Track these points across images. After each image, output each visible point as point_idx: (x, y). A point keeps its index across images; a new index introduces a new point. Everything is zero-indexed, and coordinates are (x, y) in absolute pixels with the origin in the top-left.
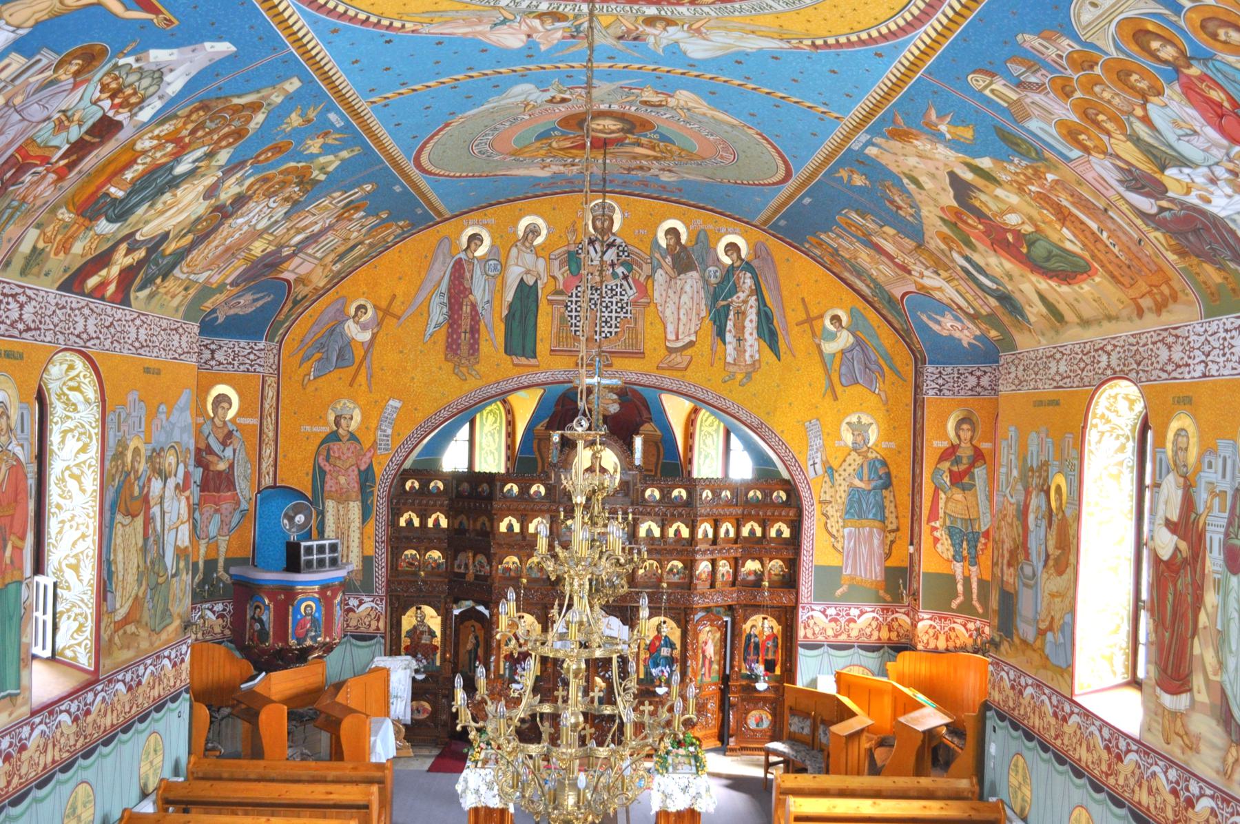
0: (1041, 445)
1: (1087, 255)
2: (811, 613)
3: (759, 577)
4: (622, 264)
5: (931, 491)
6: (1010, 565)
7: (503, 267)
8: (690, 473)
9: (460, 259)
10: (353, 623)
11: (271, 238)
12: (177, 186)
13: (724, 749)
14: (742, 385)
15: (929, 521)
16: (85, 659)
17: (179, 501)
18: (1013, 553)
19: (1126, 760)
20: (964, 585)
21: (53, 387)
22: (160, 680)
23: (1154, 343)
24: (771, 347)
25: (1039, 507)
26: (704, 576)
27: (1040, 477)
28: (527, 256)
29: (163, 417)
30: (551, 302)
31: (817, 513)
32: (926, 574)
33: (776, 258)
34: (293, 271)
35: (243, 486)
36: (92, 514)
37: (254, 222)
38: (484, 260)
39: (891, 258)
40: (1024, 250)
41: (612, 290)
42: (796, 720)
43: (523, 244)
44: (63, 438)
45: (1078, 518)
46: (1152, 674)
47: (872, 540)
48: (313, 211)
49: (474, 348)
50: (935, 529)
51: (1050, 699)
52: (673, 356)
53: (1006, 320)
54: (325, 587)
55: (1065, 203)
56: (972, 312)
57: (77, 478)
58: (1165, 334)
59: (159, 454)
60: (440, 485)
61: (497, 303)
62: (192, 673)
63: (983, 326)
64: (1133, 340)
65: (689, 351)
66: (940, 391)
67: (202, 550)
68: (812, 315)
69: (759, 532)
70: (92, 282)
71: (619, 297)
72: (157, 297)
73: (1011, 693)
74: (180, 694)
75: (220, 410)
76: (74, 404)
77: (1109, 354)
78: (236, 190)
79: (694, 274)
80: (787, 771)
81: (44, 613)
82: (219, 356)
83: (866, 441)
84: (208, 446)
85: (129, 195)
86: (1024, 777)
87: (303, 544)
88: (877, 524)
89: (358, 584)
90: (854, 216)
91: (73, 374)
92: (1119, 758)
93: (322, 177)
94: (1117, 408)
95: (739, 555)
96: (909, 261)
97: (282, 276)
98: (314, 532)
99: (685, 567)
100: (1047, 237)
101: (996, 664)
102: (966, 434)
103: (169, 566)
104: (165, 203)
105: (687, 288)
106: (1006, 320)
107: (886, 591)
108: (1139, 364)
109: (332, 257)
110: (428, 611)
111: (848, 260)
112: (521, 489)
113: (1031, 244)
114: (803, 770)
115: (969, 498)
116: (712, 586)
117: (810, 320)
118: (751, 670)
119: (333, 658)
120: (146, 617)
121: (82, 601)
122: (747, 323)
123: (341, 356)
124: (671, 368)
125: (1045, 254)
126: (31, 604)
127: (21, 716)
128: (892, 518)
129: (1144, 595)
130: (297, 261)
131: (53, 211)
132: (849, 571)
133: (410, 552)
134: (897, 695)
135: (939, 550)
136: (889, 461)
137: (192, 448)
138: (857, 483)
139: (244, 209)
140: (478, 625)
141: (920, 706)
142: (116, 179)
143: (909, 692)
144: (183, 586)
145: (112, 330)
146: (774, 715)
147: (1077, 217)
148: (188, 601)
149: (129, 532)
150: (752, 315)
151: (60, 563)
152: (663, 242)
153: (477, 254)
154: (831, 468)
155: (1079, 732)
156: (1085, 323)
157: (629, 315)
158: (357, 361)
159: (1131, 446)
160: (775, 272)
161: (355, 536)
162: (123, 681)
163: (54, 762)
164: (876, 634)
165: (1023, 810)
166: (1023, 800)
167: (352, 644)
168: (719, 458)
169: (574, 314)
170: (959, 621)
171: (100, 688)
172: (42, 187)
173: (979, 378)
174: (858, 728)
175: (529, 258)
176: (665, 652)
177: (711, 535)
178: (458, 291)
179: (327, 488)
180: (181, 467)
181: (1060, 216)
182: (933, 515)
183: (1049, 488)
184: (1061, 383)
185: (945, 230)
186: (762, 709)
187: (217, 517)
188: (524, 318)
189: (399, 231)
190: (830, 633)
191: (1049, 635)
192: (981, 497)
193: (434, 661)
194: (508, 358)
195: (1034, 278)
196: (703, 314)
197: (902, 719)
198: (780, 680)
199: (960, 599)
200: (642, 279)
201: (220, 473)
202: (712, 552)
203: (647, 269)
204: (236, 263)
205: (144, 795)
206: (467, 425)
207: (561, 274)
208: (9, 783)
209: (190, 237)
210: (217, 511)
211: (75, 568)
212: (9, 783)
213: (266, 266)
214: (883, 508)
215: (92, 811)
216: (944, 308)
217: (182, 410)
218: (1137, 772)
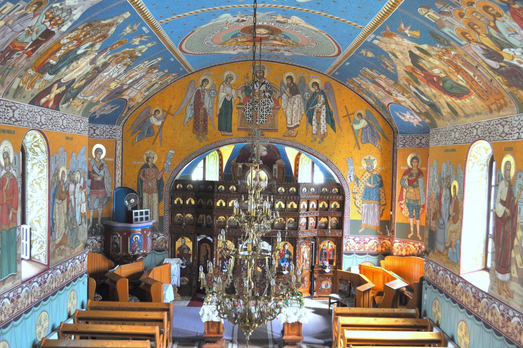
0: (447, 168)
1: (468, 87)
3: (327, 224)
4: (268, 92)
5: (400, 188)
6: (433, 219)
7: (218, 93)
8: (297, 181)
11: (118, 81)
12: (78, 59)
13: (311, 297)
14: (319, 143)
15: (399, 201)
16: (44, 260)
17: (82, 193)
18: (435, 214)
19: (482, 302)
20: (414, 228)
21: (28, 145)
22: (75, 268)
23: (497, 125)
24: (332, 127)
25: (446, 195)
26: (303, 224)
27: (447, 182)
28: (227, 88)
29: (74, 158)
30: (238, 108)
31: (351, 198)
32: (398, 223)
34: (128, 95)
35: (108, 187)
36: (45, 199)
37: (111, 74)
38: (209, 91)
39: (383, 88)
40: (441, 85)
41: (264, 103)
42: (342, 285)
44: (32, 167)
45: (463, 199)
46: (494, 265)
48: (136, 69)
49: (205, 128)
50: (402, 204)
51: (450, 276)
52: (290, 131)
53: (433, 115)
54: (143, 229)
55: (459, 64)
56: (418, 111)
57: (39, 184)
58: (501, 120)
59: (73, 174)
60: (191, 186)
61: (215, 109)
62: (88, 265)
63: (423, 117)
64: (487, 123)
65: (297, 129)
66: (404, 145)
67: (92, 214)
69: (326, 206)
70: (43, 100)
71: (267, 106)
72: (71, 107)
73: (433, 274)
74: (83, 274)
76: (37, 153)
77: (477, 129)
78: (103, 61)
79: (299, 95)
80: (338, 306)
81: (26, 241)
82: (97, 132)
83: (372, 167)
84: (93, 170)
85: (58, 63)
86: (439, 309)
87: (134, 211)
88: (377, 202)
90: (368, 70)
91: (36, 140)
92: (479, 301)
93: (140, 55)
94: (480, 152)
95: (318, 215)
96: (391, 90)
97: (124, 97)
98: (138, 206)
99: (295, 221)
100: (451, 79)
101: (427, 261)
102: (415, 164)
103: (78, 221)
104: (73, 66)
105: (296, 102)
106: (433, 115)
107: (380, 230)
108: (490, 133)
109: (144, 89)
110: (187, 240)
111: (365, 89)
112: (225, 187)
113: (444, 82)
114: (345, 306)
115: (416, 191)
116: (307, 228)
117: (348, 115)
118: (323, 263)
119: (148, 259)
120: (69, 242)
121: (42, 235)
122: (322, 117)
123: (148, 132)
124: (289, 136)
125: (450, 86)
126: (20, 237)
127: (18, 283)
128: (383, 200)
129: (491, 232)
130: (129, 91)
131: (26, 70)
132: (365, 222)
133: (178, 215)
134: (385, 274)
137: (87, 171)
139: (107, 69)
140: (208, 245)
141: (395, 279)
142: (52, 57)
143: (391, 273)
144: (84, 229)
145: (52, 121)
146: (333, 282)
147: (464, 70)
148: (86, 235)
149: (61, 207)
150: (324, 113)
151: (32, 220)
152: (285, 82)
153: (206, 88)
154: (357, 178)
155: (462, 290)
156: (467, 116)
157: (271, 114)
158: (156, 134)
159: (486, 169)
160: (334, 95)
161: (156, 208)
162: (60, 269)
163: (31, 303)
164: (376, 249)
165: (438, 322)
166: (438, 318)
167: (155, 253)
168: (309, 174)
169: (248, 113)
171: (50, 272)
172: (21, 60)
173: (421, 140)
174: (369, 288)
175: (228, 89)
176: (287, 256)
177: (306, 207)
178: (198, 104)
179: (144, 187)
180: (82, 179)
181: (457, 70)
182: (401, 198)
183: (451, 186)
184: (456, 142)
185: (407, 76)
186: (328, 280)
187: (97, 200)
189: (173, 78)
190: (356, 248)
191: (450, 249)
192: (421, 191)
193: (189, 260)
195: (445, 96)
196: (303, 113)
197: (387, 284)
198: (335, 268)
199: (412, 234)
200: (277, 98)
201: (98, 181)
202: (307, 214)
203: (279, 93)
204: (104, 92)
205: (69, 317)
206: (202, 161)
207: (242, 96)
208: (13, 311)
209: (84, 81)
210: (97, 198)
211: (39, 222)
212: (13, 311)
213: (116, 93)
214: (380, 195)
215: (47, 323)
216: (406, 109)
217: (82, 155)
218: (487, 306)
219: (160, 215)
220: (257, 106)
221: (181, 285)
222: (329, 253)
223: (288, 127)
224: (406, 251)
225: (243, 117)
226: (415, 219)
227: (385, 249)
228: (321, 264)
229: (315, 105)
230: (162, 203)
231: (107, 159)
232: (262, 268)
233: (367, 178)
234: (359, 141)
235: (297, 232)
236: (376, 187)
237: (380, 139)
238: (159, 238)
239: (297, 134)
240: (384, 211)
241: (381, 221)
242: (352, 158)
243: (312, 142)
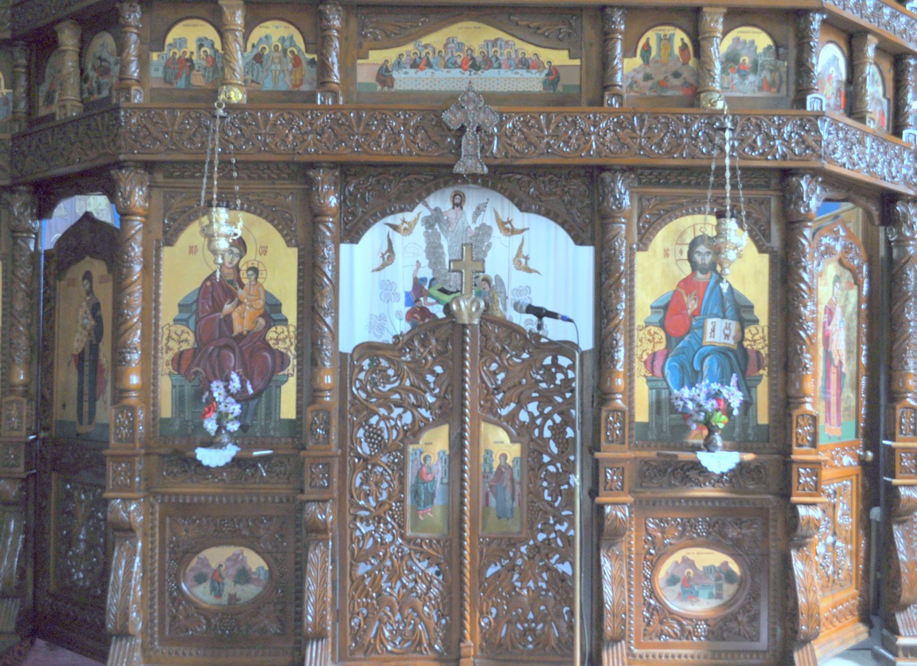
99: (778, 47)
176: (718, 331)
232: (521, 432)
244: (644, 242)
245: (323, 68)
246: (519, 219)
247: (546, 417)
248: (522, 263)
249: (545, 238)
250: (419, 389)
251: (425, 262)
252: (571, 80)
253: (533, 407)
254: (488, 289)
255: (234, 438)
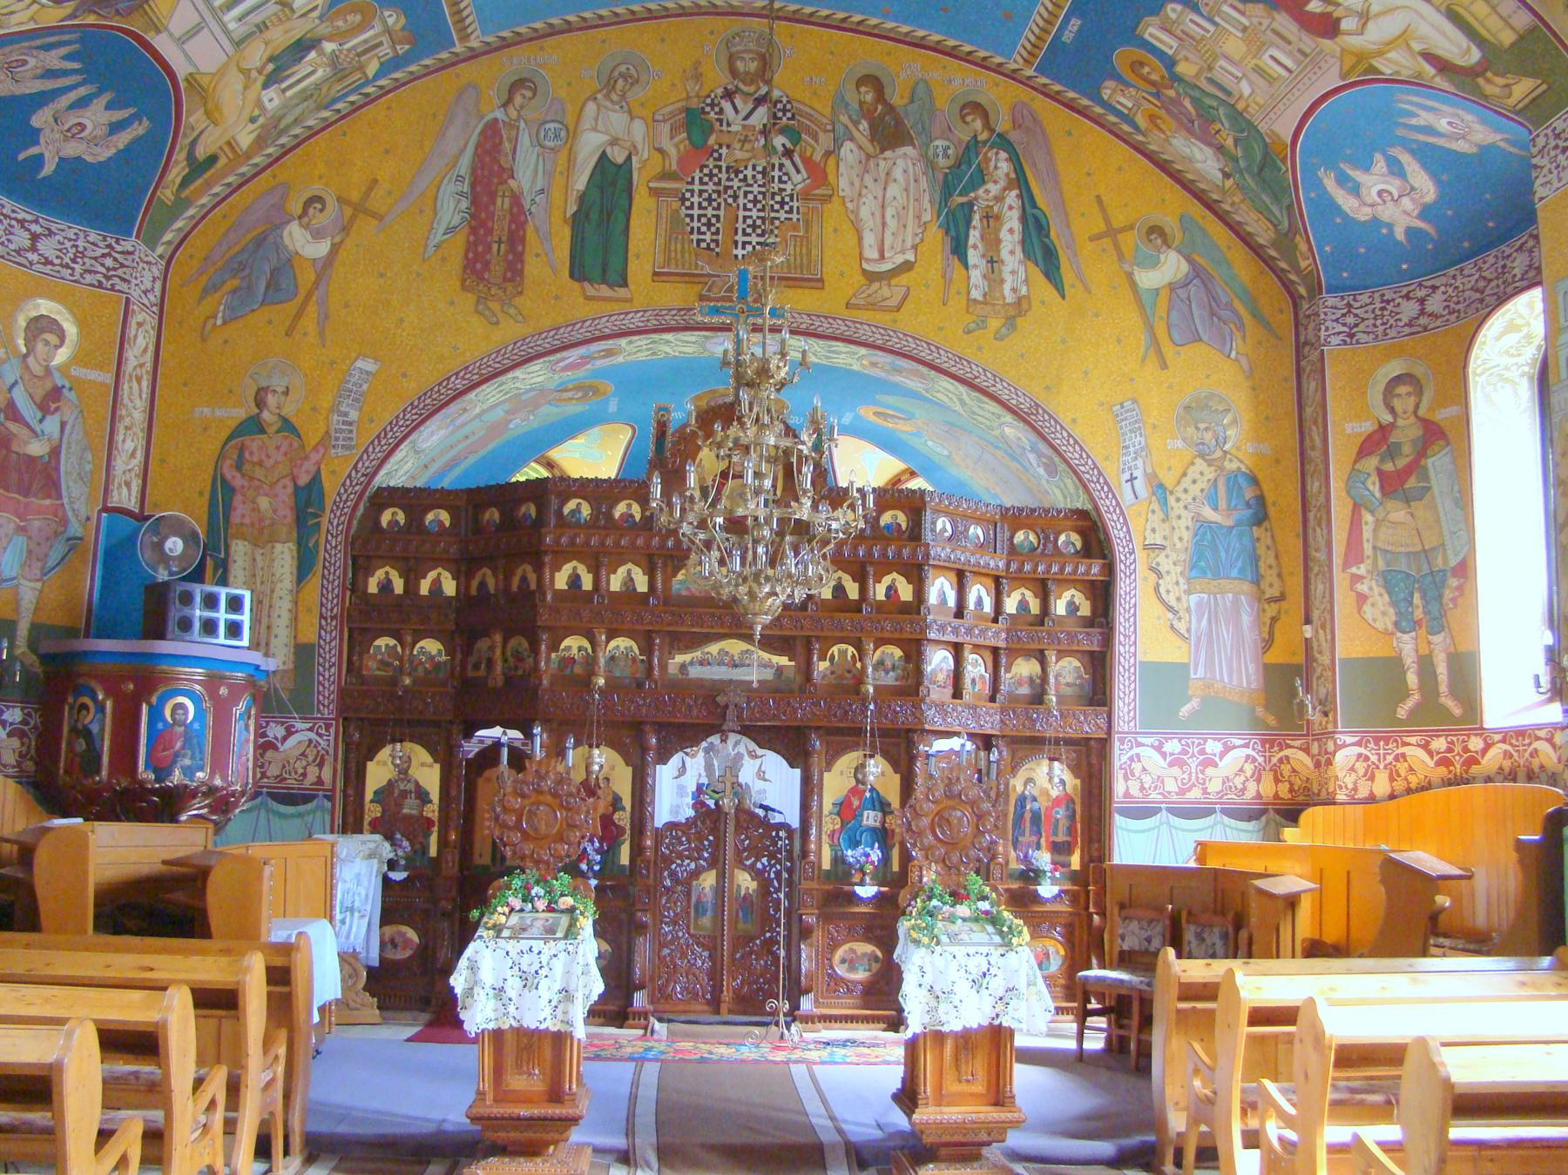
2: (1136, 750)
4: (782, 131)
5: (1348, 510)
7: (572, 134)
9: (496, 120)
10: (273, 771)
14: (999, 337)
15: (1346, 565)
20: (1420, 674)
24: (1047, 275)
26: (941, 677)
32: (1346, 662)
33: (1049, 130)
35: (75, 492)
42: (1134, 926)
43: (607, 96)
47: (1238, 613)
49: (515, 271)
50: (1357, 578)
52: (875, 286)
60: (445, 517)
65: (905, 279)
66: (1351, 336)
68: (1116, 225)
75: (40, 346)
79: (909, 150)
82: (47, 247)
88: (1246, 587)
89: (284, 695)
95: (1002, 644)
99: (907, 658)
102: (1404, 403)
105: (898, 173)
107: (1266, 708)
110: (420, 754)
116: (957, 694)
122: (1004, 234)
123: (273, 284)
124: (872, 306)
128: (1270, 576)
132: (1201, 673)
133: (383, 642)
135: (1368, 616)
136: (1260, 476)
138: (1208, 513)
152: (852, 97)
154: (1161, 486)
157: (795, 216)
158: (303, 292)
160: (1050, 153)
161: (283, 607)
164: (1252, 788)
169: (696, 212)
170: (1413, 740)
173: (1422, 301)
176: (870, 818)
177: (952, 602)
178: (489, 172)
179: (236, 518)
182: (1354, 553)
187: (20, 542)
188: (607, 216)
190: (1171, 786)
194: (576, 285)
196: (927, 217)
200: (817, 157)
201: (32, 460)
203: (825, 141)
207: (674, 146)
210: (22, 530)
214: (1255, 559)
219: (303, 639)
220: (736, 183)
221: (382, 960)
222: (1049, 816)
223: (864, 270)
224: (1392, 779)
225: (676, 228)
226: (1423, 631)
227: (1291, 790)
228: (1015, 866)
229: (975, 189)
230: (314, 583)
231: (76, 371)
232: (758, 875)
233: (1199, 486)
234: (1161, 333)
235: (917, 706)
236: (1239, 523)
237: (1241, 327)
238: (292, 741)
239: (905, 298)
240: (1278, 625)
241: (1266, 666)
242: (1134, 401)
243: (969, 332)
244: (829, 767)
245: (650, 668)
246: (760, 752)
247: (772, 866)
248: (761, 775)
249: (773, 762)
250: (700, 850)
251: (704, 774)
252: (791, 674)
253: (764, 860)
254: (739, 790)
255: (596, 875)
